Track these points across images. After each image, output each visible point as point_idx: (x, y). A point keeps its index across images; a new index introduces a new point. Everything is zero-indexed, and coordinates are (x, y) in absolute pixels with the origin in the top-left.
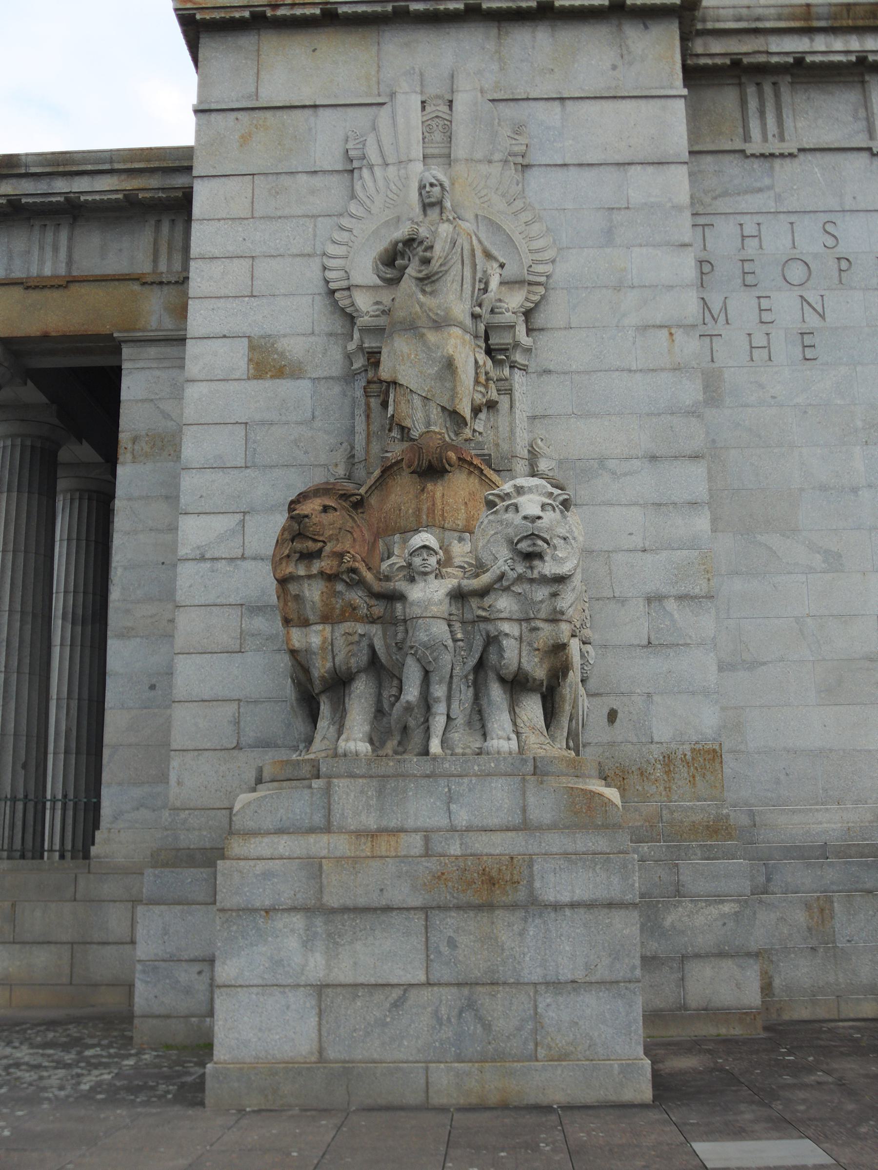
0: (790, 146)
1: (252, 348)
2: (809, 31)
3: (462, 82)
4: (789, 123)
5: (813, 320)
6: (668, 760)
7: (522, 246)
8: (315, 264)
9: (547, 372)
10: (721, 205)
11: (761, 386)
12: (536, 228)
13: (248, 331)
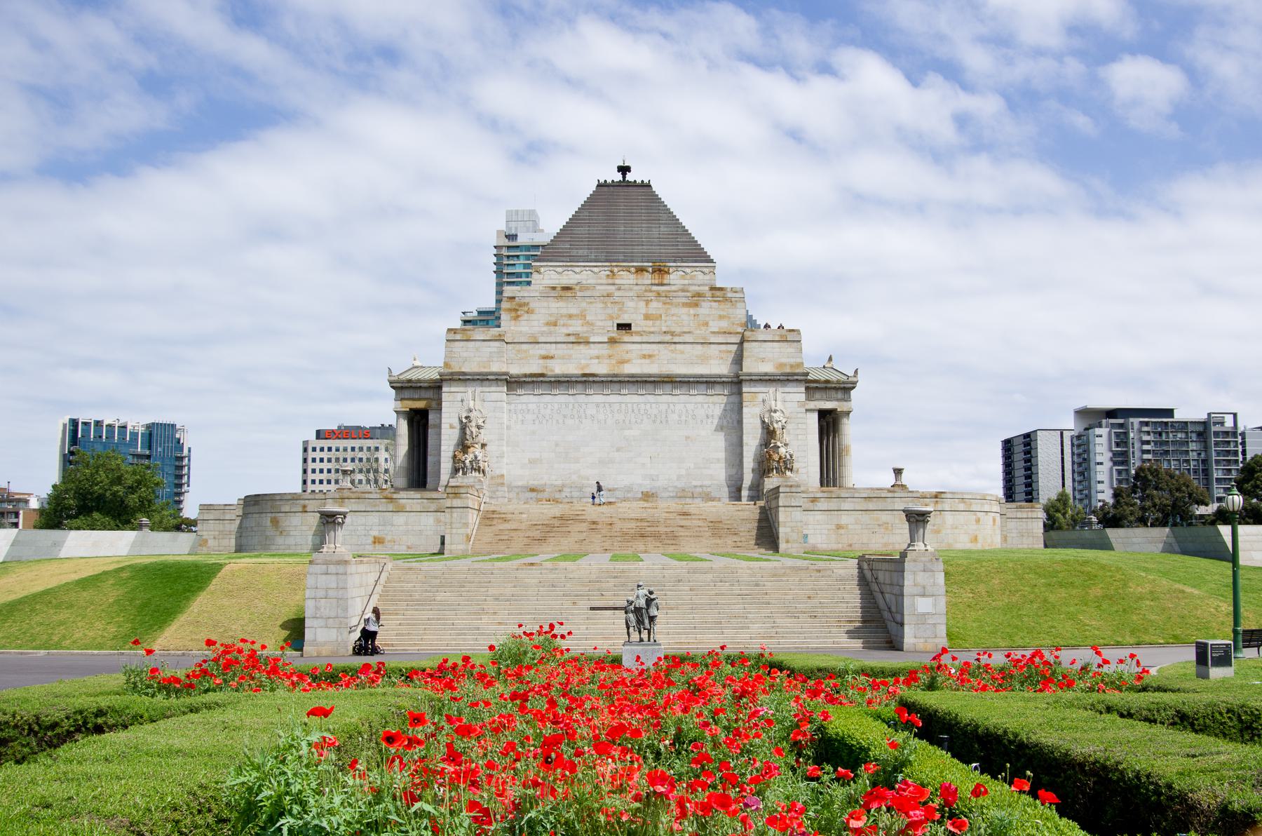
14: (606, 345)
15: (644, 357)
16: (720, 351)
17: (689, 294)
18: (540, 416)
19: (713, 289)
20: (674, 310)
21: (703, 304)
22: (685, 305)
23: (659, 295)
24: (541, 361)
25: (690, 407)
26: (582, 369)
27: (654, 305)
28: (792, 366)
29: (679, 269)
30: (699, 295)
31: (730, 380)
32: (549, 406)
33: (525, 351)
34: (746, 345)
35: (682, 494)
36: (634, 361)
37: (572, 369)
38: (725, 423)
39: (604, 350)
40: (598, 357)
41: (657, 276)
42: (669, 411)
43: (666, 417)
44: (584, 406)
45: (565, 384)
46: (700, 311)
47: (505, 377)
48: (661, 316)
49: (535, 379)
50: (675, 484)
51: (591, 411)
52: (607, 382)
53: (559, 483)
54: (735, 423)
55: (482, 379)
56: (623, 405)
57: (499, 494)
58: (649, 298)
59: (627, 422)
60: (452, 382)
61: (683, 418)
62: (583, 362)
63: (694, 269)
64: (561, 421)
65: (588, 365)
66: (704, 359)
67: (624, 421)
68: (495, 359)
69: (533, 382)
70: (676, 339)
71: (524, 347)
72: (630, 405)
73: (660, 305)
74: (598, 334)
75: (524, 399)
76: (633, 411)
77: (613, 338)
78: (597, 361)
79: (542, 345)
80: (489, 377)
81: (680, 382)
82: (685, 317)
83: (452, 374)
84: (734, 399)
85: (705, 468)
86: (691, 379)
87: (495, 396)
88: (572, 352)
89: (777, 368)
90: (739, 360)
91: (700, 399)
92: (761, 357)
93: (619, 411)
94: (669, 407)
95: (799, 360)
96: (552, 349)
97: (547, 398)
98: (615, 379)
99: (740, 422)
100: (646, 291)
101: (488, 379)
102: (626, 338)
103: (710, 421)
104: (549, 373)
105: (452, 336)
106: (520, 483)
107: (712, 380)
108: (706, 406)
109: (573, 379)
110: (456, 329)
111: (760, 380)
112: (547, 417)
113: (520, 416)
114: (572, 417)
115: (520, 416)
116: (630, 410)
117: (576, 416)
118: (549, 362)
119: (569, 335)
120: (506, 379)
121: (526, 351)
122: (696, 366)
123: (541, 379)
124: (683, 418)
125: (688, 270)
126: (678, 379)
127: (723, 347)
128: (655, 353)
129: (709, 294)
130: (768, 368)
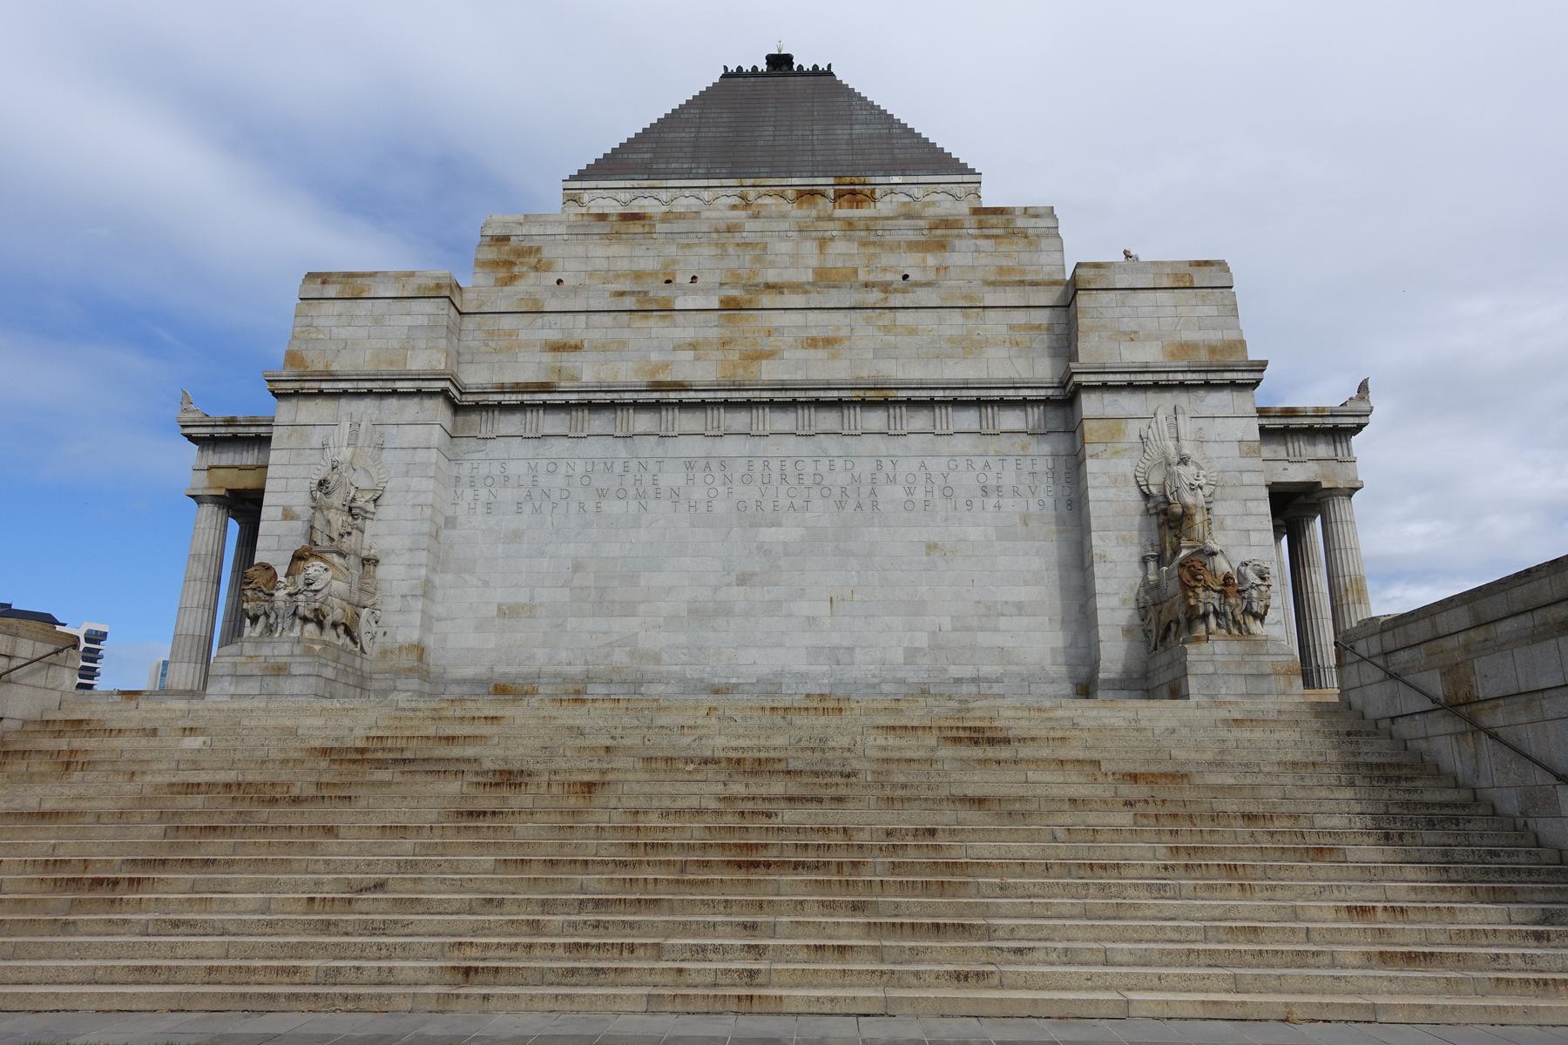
1: (284, 510)
4: (496, 426)
5: (492, 499)
6: (400, 648)
8: (308, 481)
10: (466, 456)
11: (470, 522)
12: (381, 471)
13: (283, 503)
15: (813, 343)
16: (1011, 327)
24: (548, 358)
25: (937, 466)
28: (1213, 350)
31: (1042, 392)
32: (563, 468)
33: (510, 334)
34: (1083, 300)
37: (625, 372)
38: (1034, 506)
39: (711, 330)
42: (881, 477)
43: (873, 492)
44: (652, 465)
47: (442, 384)
49: (526, 397)
50: (900, 675)
51: (672, 477)
52: (715, 404)
53: (577, 669)
55: (382, 389)
56: (758, 465)
59: (768, 506)
61: (919, 494)
67: (759, 504)
68: (421, 344)
70: (896, 300)
71: (507, 322)
72: (775, 465)
76: (784, 478)
77: (734, 299)
79: (552, 317)
80: (399, 385)
85: (982, 629)
86: (938, 394)
87: (412, 435)
89: (1173, 355)
90: (1066, 343)
91: (964, 444)
92: (1124, 328)
93: (747, 479)
94: (880, 465)
95: (1230, 335)
96: (577, 328)
102: (767, 300)
104: (564, 385)
105: (315, 290)
106: (469, 672)
108: (979, 463)
109: (628, 397)
110: (330, 274)
113: (483, 494)
114: (621, 495)
115: (483, 494)
116: (776, 476)
117: (632, 493)
118: (569, 360)
119: (622, 294)
120: (444, 393)
121: (510, 333)
123: (545, 397)
124: (919, 494)
127: (1020, 317)
130: (1147, 354)
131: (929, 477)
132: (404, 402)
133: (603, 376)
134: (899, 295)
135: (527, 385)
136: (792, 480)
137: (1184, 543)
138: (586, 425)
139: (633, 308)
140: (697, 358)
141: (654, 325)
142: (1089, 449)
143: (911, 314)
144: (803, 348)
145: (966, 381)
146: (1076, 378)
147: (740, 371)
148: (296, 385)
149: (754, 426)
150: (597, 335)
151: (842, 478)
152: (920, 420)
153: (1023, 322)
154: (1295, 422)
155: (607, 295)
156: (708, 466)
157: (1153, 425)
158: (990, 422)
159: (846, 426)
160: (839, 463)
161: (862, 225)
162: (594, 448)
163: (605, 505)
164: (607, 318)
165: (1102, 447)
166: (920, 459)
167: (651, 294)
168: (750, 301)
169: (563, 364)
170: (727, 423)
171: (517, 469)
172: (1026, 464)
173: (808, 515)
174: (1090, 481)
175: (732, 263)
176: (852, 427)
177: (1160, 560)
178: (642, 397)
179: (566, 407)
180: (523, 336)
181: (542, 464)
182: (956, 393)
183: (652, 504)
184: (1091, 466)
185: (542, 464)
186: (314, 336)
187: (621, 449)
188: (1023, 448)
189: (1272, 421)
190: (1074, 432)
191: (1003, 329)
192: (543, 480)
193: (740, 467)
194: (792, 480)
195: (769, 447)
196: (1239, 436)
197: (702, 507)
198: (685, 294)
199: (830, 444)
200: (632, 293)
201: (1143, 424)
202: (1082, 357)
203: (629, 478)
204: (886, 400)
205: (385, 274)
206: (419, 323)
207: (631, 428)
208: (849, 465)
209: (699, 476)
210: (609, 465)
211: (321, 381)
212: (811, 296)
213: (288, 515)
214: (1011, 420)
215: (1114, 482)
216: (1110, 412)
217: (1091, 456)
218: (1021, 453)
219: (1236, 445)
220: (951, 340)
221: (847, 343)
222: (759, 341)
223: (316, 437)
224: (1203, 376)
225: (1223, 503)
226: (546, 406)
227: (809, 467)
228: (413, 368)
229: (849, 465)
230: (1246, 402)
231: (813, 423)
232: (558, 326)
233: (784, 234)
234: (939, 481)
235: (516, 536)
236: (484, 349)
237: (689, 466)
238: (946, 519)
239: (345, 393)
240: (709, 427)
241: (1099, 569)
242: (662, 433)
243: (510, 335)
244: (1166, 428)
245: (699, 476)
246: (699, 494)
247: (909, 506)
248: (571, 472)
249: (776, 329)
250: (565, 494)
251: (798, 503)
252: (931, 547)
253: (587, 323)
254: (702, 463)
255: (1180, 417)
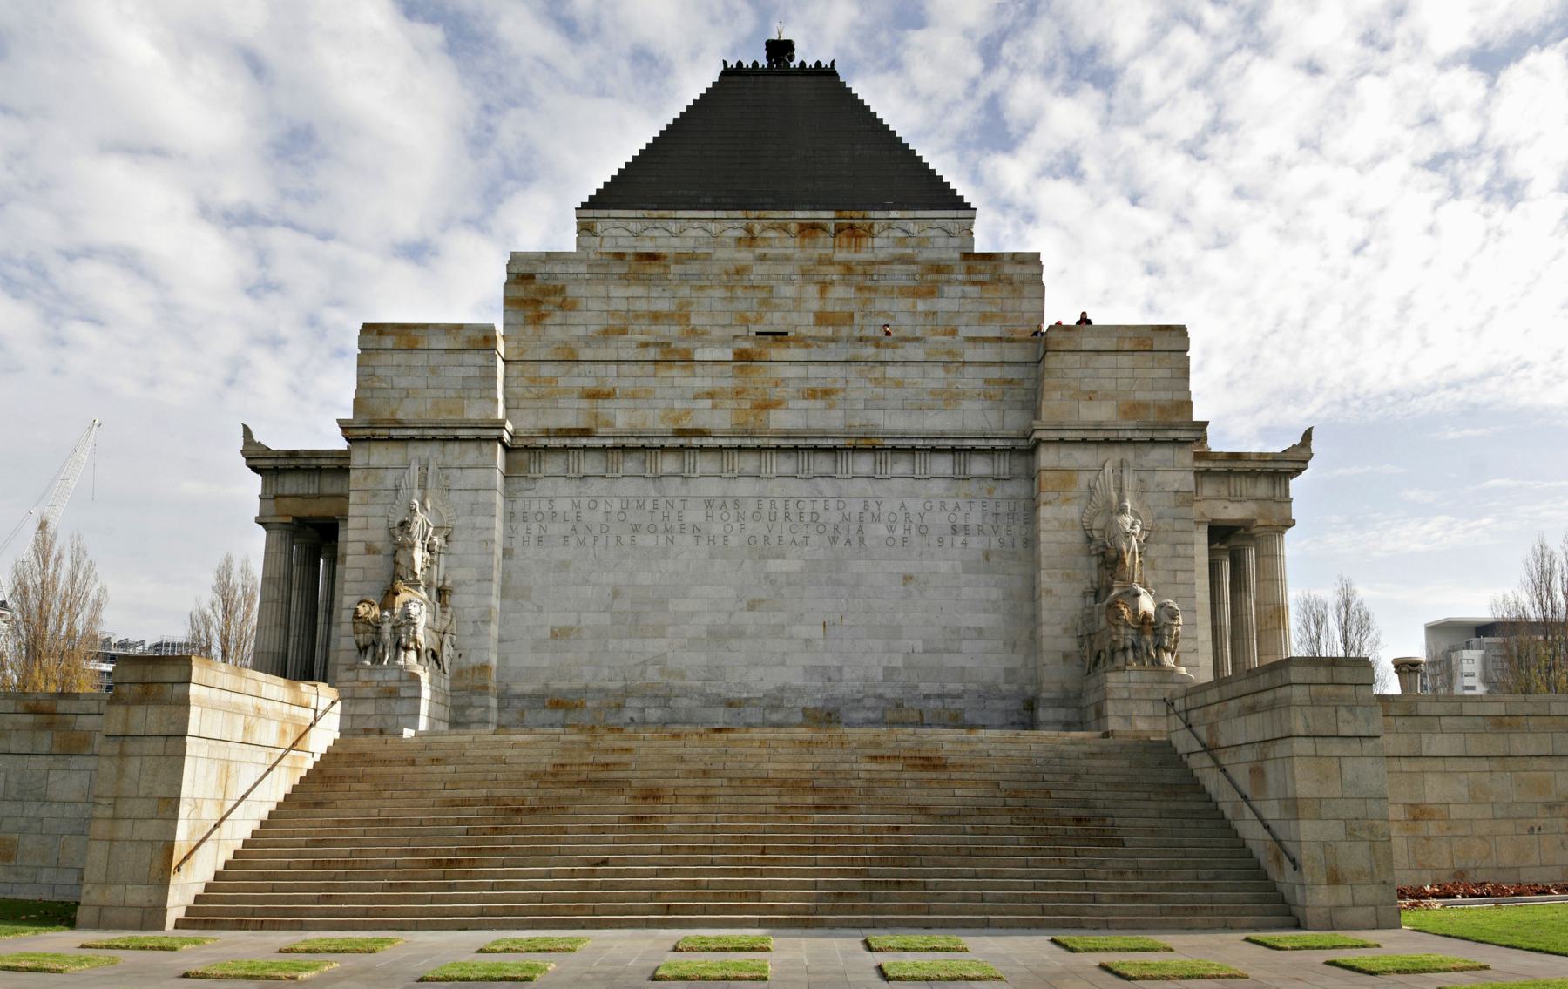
0: (541, 475)
1: (367, 545)
2: (548, 437)
3: (431, 462)
4: (543, 467)
5: (543, 533)
7: (445, 515)
9: (450, 554)
10: (519, 494)
14: (728, 368)
15: (812, 394)
16: (987, 381)
17: (914, 268)
18: (580, 528)
19: (969, 256)
20: (882, 304)
21: (946, 288)
22: (906, 292)
23: (848, 268)
24: (585, 403)
25: (914, 506)
26: (677, 420)
27: (839, 292)
29: (895, 224)
30: (939, 268)
31: (1009, 443)
32: (602, 507)
35: (897, 713)
36: (792, 404)
37: (651, 418)
38: (995, 544)
39: (726, 381)
40: (711, 395)
41: (845, 241)
42: (868, 516)
43: (860, 530)
44: (678, 505)
45: (636, 455)
46: (942, 305)
48: (851, 316)
49: (568, 441)
54: (1019, 544)
56: (766, 504)
57: (475, 713)
58: (828, 278)
59: (774, 541)
60: (373, 445)
61: (899, 532)
62: (678, 404)
63: (927, 223)
64: (626, 539)
65: (689, 412)
66: (949, 398)
68: (475, 393)
69: (565, 449)
70: (887, 354)
71: (547, 371)
72: (780, 504)
73: (850, 292)
74: (712, 343)
75: (545, 487)
76: (787, 516)
78: (708, 403)
80: (460, 433)
81: (894, 449)
82: (905, 319)
83: (372, 425)
84: (1018, 488)
86: (920, 443)
87: (473, 477)
88: (652, 382)
90: (1032, 405)
91: (938, 487)
93: (756, 517)
94: (866, 505)
97: (598, 486)
98: (748, 442)
99: (1031, 542)
100: (820, 262)
101: (456, 439)
102: (775, 353)
103: (959, 539)
104: (602, 431)
107: (968, 443)
109: (656, 442)
111: (1084, 441)
112: (597, 530)
113: (535, 527)
115: (535, 527)
116: (781, 515)
117: (661, 528)
118: (605, 407)
119: (645, 345)
121: (551, 381)
122: (931, 413)
123: (584, 441)
124: (899, 532)
125: (913, 227)
126: (888, 443)
127: (995, 373)
128: (840, 384)
129: (961, 267)
131: (907, 517)
132: (465, 446)
133: (633, 421)
134: (889, 351)
135: (569, 430)
136: (794, 518)
137: (1116, 583)
138: (621, 467)
139: (658, 358)
140: (714, 407)
141: (676, 373)
142: (1044, 497)
143: (900, 368)
144: (804, 398)
145: (942, 432)
146: (1037, 435)
147: (752, 419)
148: (368, 432)
149: (763, 470)
150: (626, 384)
151: (835, 517)
152: (902, 466)
153: (997, 377)
154: (1238, 465)
155: (634, 345)
156: (724, 504)
157: (1100, 477)
158: (962, 467)
159: (839, 469)
160: (832, 503)
161: (859, 269)
162: (629, 488)
163: (639, 538)
164: (635, 369)
165: (1054, 495)
166: (900, 501)
167: (673, 346)
168: (760, 354)
169: (599, 410)
170: (741, 466)
171: (563, 505)
172: (990, 505)
173: (807, 548)
174: (1043, 525)
175: (741, 306)
176: (844, 472)
177: (1097, 594)
178: (670, 442)
179: (604, 449)
180: (562, 383)
181: (584, 502)
182: (934, 443)
183: (678, 538)
184: (1045, 512)
185: (584, 502)
186: (377, 385)
187: (651, 489)
188: (990, 492)
189: (1217, 464)
190: (1033, 479)
191: (979, 383)
192: (586, 516)
193: (751, 507)
194: (794, 518)
195: (775, 488)
196: (1176, 486)
197: (720, 541)
198: (703, 347)
199: (825, 486)
200: (656, 344)
201: (1092, 476)
202: (1044, 414)
203: (658, 515)
204: (874, 447)
205: (436, 326)
206: (471, 374)
207: (659, 470)
208: (841, 505)
209: (717, 513)
210: (641, 503)
211: (390, 428)
212: (812, 349)
213: (370, 550)
214: (979, 466)
215: (1063, 526)
216: (1065, 464)
217: (1045, 503)
218: (987, 496)
219: (1172, 495)
220: (933, 393)
221: (842, 394)
222: (768, 391)
223: (390, 478)
224: (1149, 434)
225: (1154, 546)
226: (585, 448)
227: (807, 507)
228: (471, 417)
229: (841, 505)
230: (1185, 457)
231: (811, 467)
232: (592, 374)
233: (787, 277)
234: (916, 520)
235: (564, 566)
236: (528, 395)
237: (709, 504)
238: (921, 554)
239: (412, 439)
240: (725, 470)
241: (1046, 602)
242: (686, 474)
243: (550, 383)
244: (1112, 480)
245: (717, 513)
246: (717, 529)
247: (890, 542)
248: (609, 509)
249: (783, 380)
250: (605, 528)
251: (799, 538)
252: (907, 578)
253: (617, 372)
254: (719, 502)
255: (1125, 470)
